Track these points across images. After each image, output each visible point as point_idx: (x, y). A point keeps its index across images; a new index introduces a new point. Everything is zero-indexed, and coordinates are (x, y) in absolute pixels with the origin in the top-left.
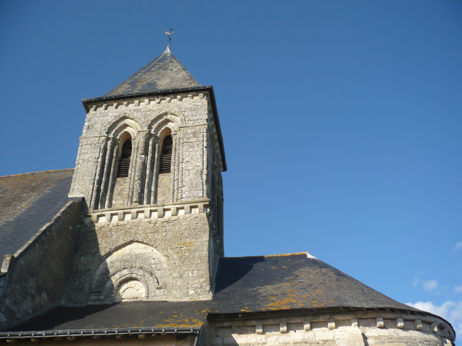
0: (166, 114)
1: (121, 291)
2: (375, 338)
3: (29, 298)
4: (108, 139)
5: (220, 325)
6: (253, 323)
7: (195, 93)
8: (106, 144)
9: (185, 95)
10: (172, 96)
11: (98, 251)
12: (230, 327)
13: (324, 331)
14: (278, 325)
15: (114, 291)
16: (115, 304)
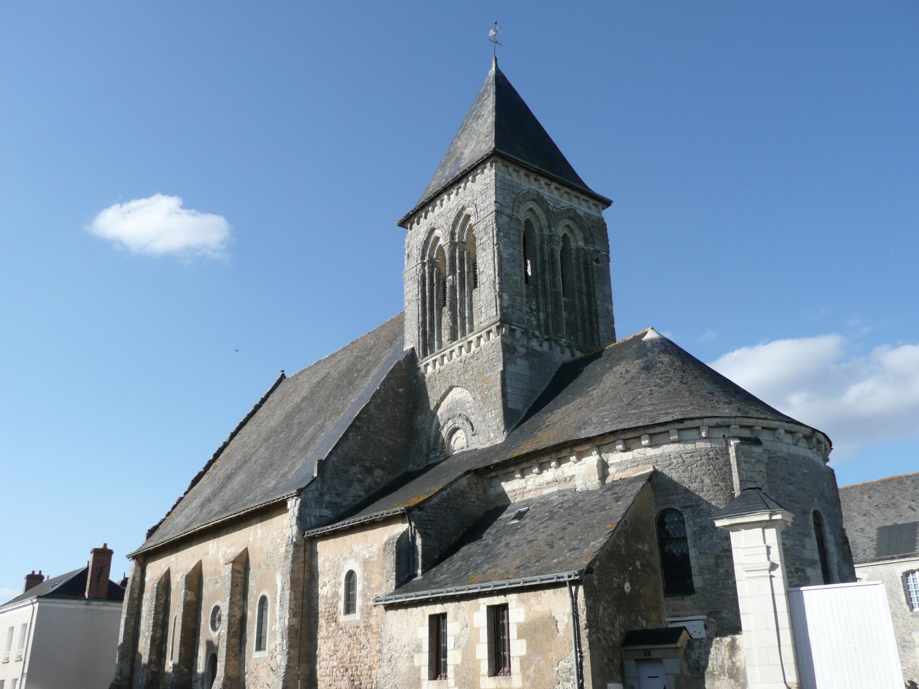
0: (464, 208)
1: (452, 443)
2: (618, 464)
3: (355, 484)
4: (424, 264)
5: (489, 476)
6: (512, 469)
7: (482, 166)
8: (424, 271)
9: (475, 173)
10: (465, 180)
11: (429, 407)
12: (497, 476)
13: (570, 466)
14: (639, 437)
15: (446, 446)
16: (447, 458)
